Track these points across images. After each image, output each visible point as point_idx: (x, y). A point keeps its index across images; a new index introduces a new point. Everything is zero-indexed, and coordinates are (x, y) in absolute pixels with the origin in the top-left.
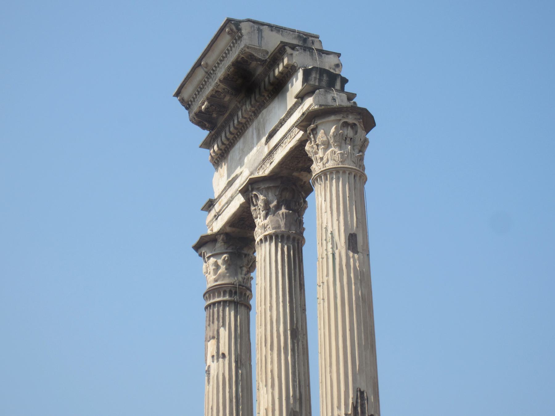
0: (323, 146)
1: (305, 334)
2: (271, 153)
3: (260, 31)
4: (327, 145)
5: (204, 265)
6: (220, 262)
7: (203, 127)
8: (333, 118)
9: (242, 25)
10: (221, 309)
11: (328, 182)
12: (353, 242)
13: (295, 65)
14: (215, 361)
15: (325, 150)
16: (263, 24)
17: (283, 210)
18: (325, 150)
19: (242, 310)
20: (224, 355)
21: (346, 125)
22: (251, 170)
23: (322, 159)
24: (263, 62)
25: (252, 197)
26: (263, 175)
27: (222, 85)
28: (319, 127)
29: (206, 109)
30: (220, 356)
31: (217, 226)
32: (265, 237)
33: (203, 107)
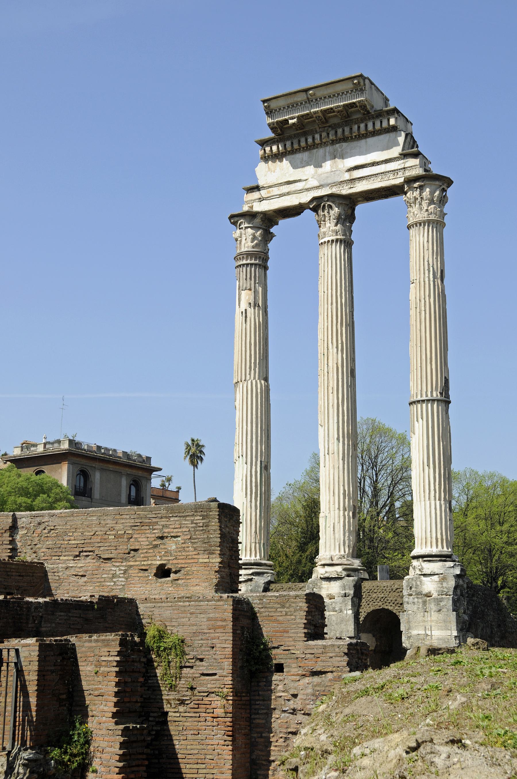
0: (428, 201)
2: (352, 181)
5: (238, 231)
7: (273, 132)
8: (437, 183)
10: (253, 269)
11: (426, 227)
13: (398, 127)
14: (252, 308)
15: (429, 204)
18: (429, 204)
20: (259, 306)
22: (322, 183)
23: (427, 210)
25: (324, 206)
26: (338, 192)
27: (320, 114)
28: (426, 186)
29: (294, 124)
31: (258, 207)
32: (337, 240)
33: (291, 122)
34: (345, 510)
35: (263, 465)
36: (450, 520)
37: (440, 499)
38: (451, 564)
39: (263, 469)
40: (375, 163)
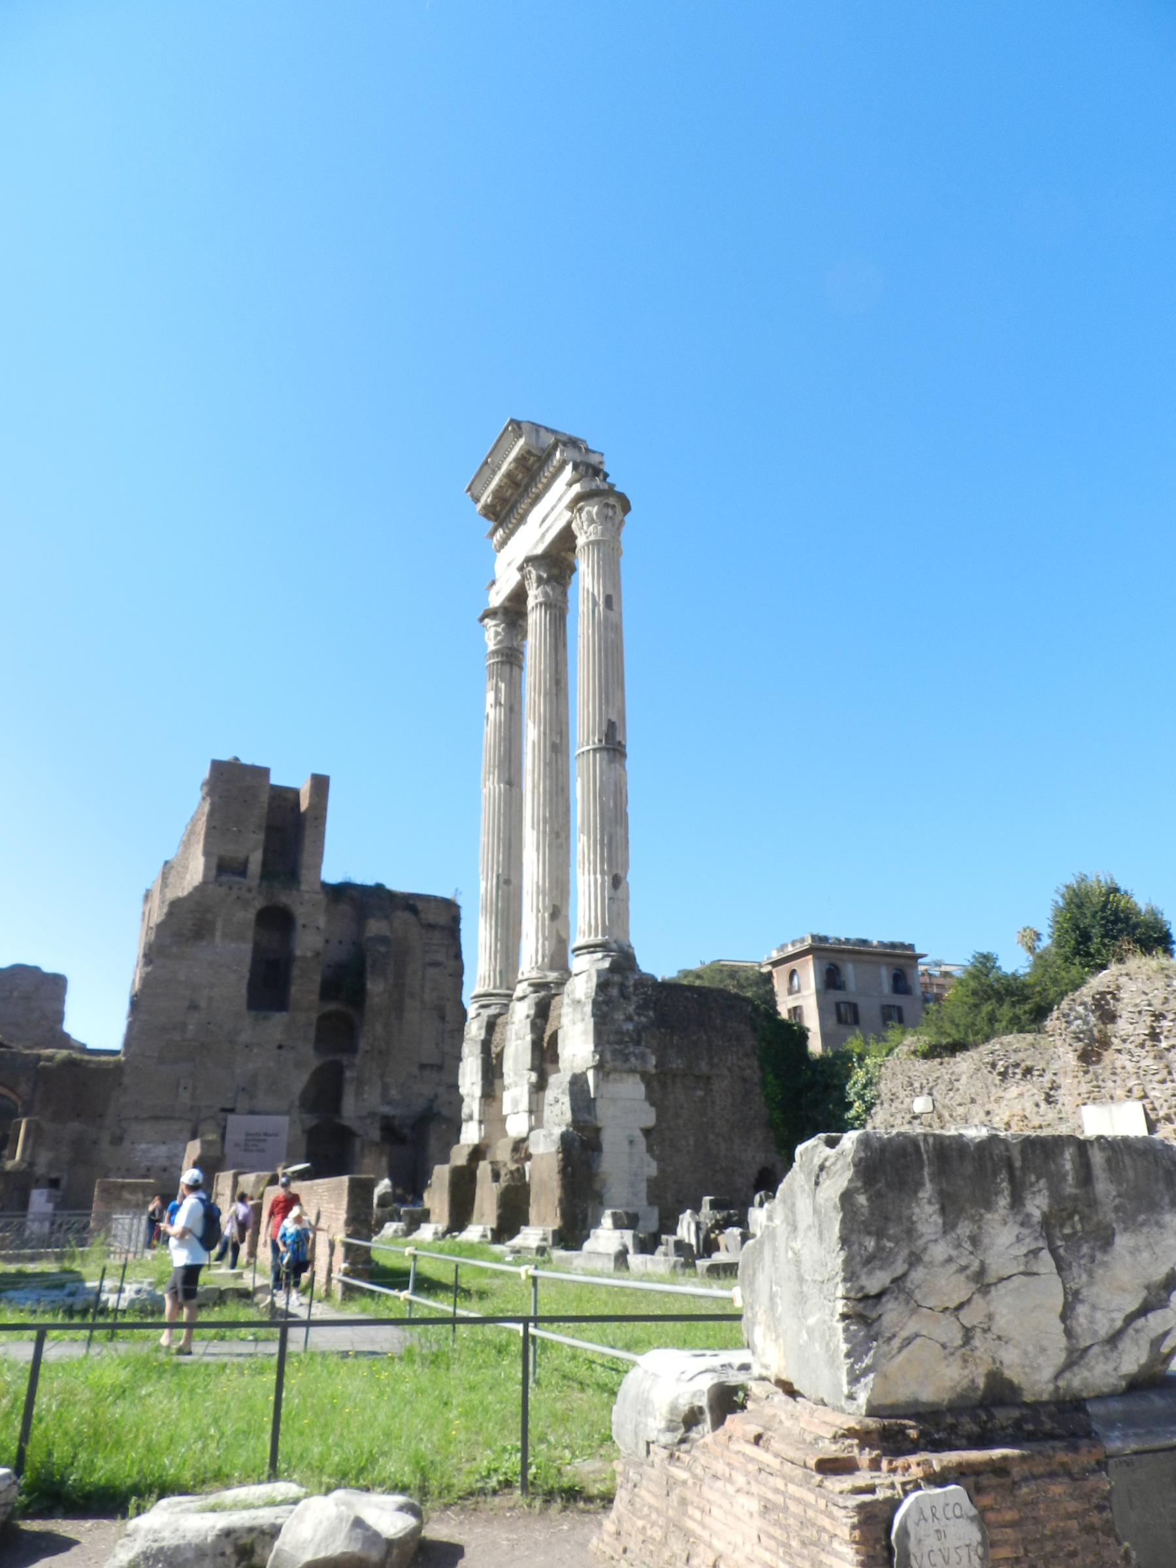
1: (566, 684)
2: (543, 536)
3: (537, 432)
6: (500, 630)
7: (489, 518)
8: (596, 499)
12: (609, 601)
15: (589, 526)
16: (539, 426)
18: (589, 526)
19: (516, 669)
21: (607, 505)
24: (539, 458)
30: (497, 703)
34: (538, 911)
35: (501, 880)
36: (610, 899)
37: (595, 873)
38: (600, 955)
39: (501, 884)
40: (553, 509)
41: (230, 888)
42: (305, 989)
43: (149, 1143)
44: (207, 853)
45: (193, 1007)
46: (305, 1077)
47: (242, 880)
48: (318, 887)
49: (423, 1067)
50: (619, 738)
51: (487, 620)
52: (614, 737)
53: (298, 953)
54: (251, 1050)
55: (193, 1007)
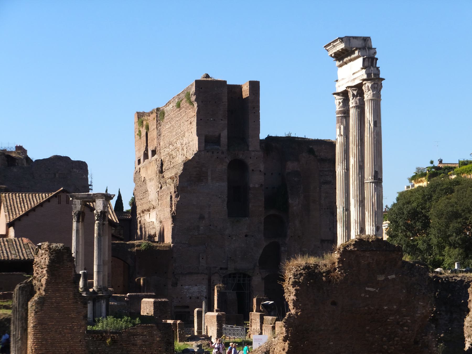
2: (354, 79)
3: (349, 40)
4: (369, 90)
6: (341, 101)
9: (343, 39)
17: (358, 98)
30: (340, 135)
41: (213, 152)
42: (256, 204)
43: (189, 285)
44: (198, 135)
45: (202, 218)
46: (261, 251)
47: (218, 147)
48: (258, 148)
49: (323, 241)
50: (379, 177)
51: (335, 96)
52: (377, 177)
53: (251, 186)
54: (232, 239)
55: (202, 218)
